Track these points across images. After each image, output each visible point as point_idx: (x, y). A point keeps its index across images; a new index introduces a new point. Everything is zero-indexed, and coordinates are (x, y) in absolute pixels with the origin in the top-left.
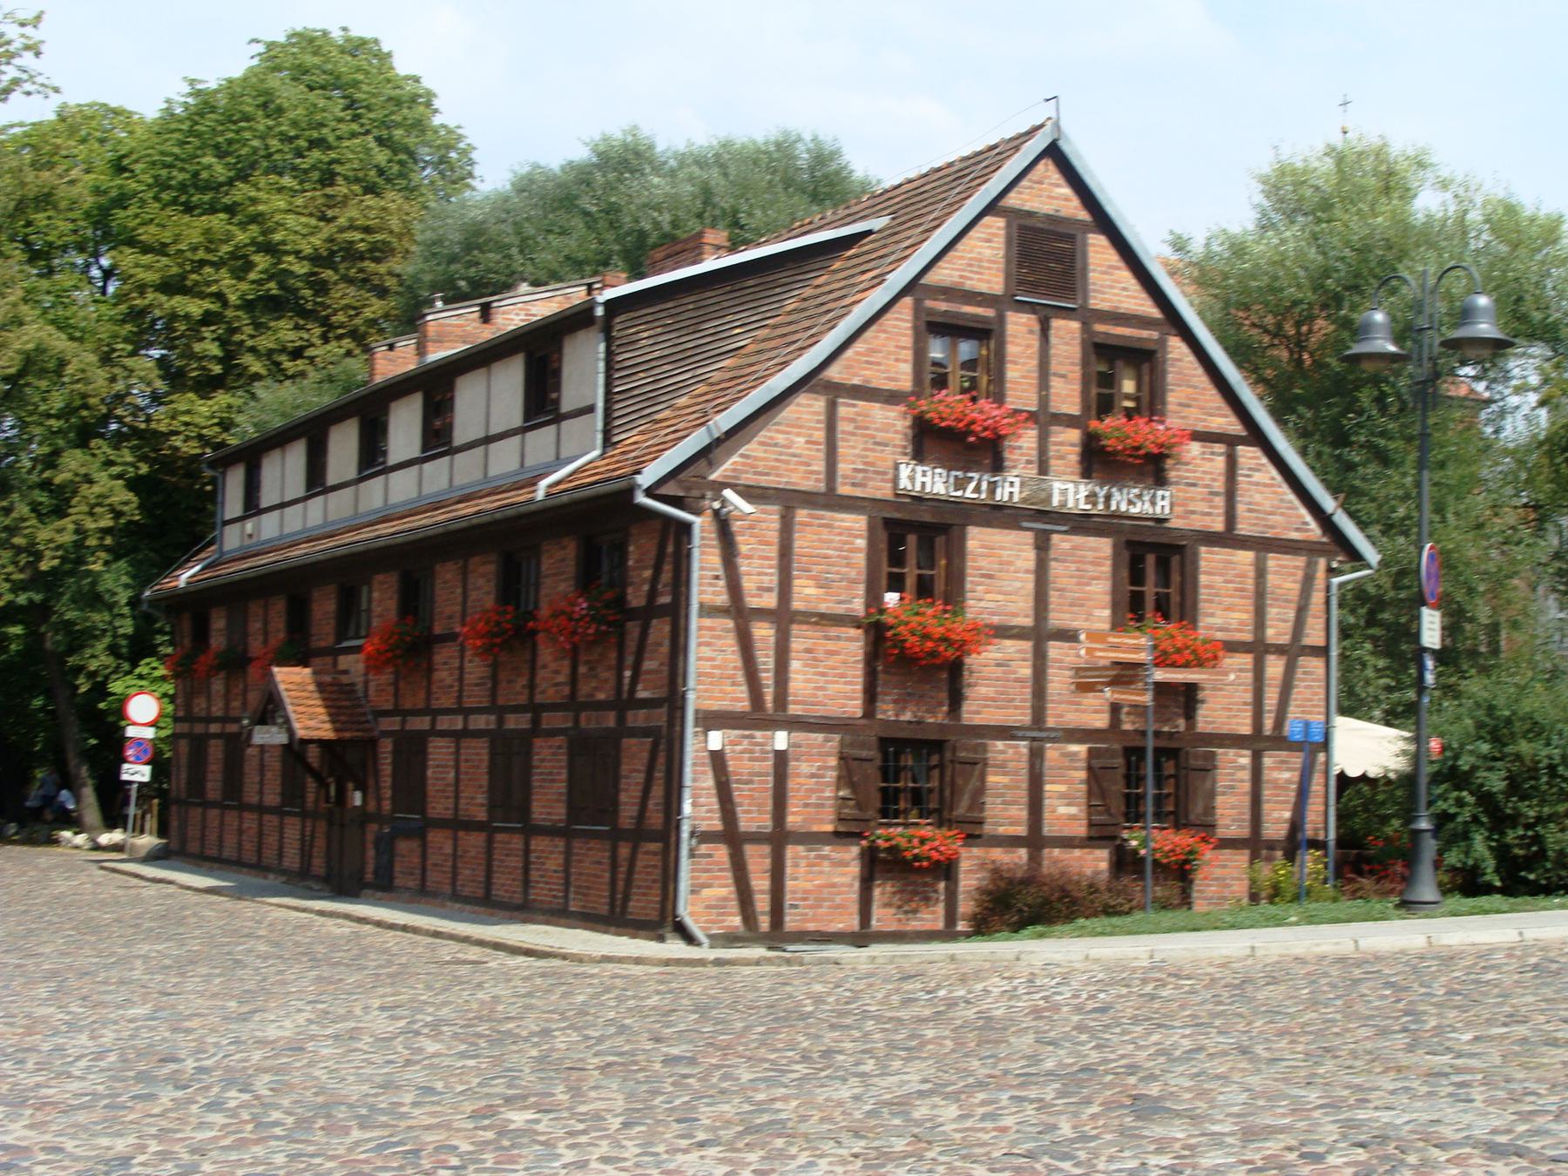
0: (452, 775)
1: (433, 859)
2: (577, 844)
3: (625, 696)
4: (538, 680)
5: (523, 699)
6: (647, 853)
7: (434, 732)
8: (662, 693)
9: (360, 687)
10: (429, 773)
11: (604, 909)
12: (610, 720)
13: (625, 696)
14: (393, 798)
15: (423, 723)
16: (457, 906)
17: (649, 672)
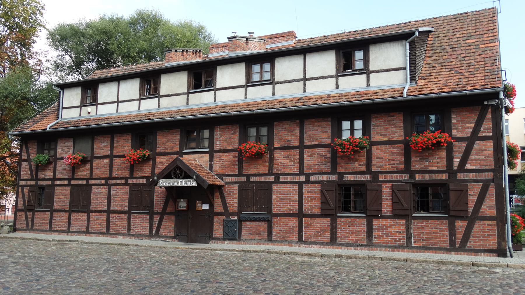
0: (296, 197)
1: (276, 228)
2: (415, 222)
3: (455, 168)
4: (373, 162)
5: (363, 169)
6: (485, 225)
7: (277, 180)
8: (493, 167)
9: (206, 167)
10: (274, 197)
11: (447, 245)
12: (444, 177)
13: (455, 168)
14: (239, 206)
15: (271, 179)
16: (302, 246)
17: (475, 160)
